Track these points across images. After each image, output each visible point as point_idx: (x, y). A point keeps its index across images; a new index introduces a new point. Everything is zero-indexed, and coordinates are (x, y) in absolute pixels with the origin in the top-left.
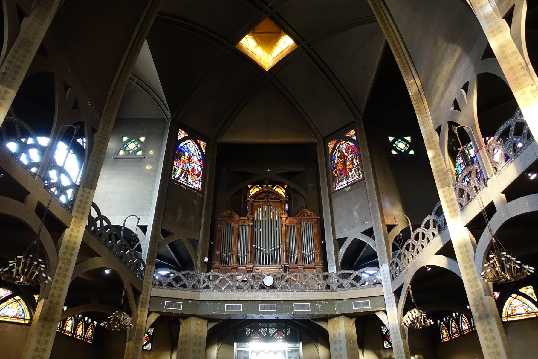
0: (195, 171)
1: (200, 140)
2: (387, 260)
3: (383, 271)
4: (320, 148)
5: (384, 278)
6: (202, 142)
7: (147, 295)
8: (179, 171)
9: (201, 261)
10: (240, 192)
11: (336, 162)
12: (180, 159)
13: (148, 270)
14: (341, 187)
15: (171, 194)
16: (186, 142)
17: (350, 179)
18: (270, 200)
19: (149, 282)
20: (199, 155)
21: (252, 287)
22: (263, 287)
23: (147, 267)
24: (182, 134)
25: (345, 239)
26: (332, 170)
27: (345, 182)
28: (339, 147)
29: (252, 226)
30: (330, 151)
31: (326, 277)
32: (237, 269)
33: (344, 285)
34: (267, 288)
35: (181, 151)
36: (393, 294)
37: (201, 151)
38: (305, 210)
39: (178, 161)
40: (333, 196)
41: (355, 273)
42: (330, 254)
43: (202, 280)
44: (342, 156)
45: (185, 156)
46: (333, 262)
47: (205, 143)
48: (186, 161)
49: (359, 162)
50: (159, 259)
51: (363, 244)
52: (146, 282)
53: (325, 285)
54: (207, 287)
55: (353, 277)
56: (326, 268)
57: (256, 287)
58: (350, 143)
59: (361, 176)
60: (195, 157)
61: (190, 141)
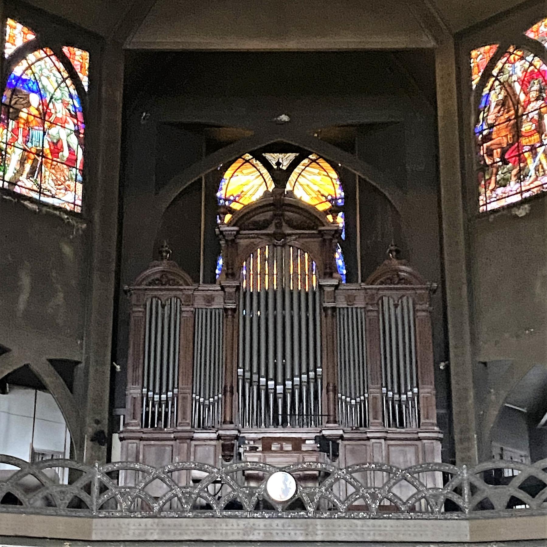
0: (61, 150)
6: (78, 52)
12: (16, 118)
14: (503, 203)
16: (31, 57)
17: (528, 180)
18: (289, 231)
20: (71, 96)
27: (513, 186)
28: (501, 71)
30: (476, 78)
38: (395, 262)
39: (12, 124)
45: (28, 105)
47: (86, 55)
53: (442, 499)
58: (538, 62)
60: (59, 105)
61: (40, 53)
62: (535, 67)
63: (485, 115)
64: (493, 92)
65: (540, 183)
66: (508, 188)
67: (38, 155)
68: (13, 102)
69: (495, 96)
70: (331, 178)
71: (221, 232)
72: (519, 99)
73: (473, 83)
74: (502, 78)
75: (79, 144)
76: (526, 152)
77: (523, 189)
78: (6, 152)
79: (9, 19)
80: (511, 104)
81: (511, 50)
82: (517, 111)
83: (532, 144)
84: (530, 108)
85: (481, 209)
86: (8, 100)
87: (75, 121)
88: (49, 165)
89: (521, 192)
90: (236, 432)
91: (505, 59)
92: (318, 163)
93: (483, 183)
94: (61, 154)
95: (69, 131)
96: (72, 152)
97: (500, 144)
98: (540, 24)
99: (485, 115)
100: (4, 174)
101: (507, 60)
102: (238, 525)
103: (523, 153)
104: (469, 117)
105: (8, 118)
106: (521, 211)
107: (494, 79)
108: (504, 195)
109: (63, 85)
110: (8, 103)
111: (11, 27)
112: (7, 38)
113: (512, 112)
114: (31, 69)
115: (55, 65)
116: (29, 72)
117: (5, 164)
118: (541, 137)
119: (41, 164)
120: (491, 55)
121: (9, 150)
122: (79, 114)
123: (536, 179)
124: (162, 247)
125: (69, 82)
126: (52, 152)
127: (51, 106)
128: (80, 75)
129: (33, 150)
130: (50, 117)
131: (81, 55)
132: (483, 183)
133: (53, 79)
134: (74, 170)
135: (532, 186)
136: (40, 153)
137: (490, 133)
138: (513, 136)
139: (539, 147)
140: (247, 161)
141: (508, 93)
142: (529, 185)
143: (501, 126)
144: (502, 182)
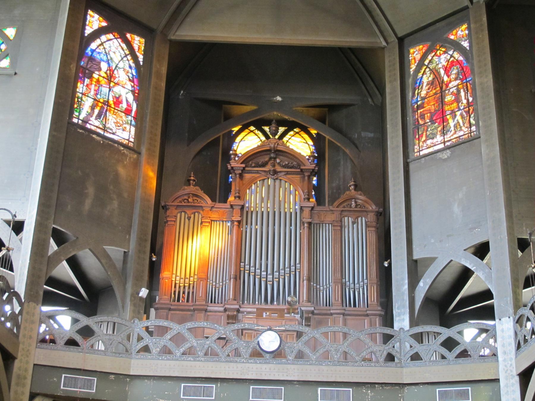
0: (121, 102)
2: (511, 310)
3: (503, 331)
7: (27, 362)
8: (88, 103)
9: (132, 295)
10: (215, 143)
11: (423, 93)
12: (91, 77)
13: (28, 313)
14: (431, 150)
16: (104, 38)
18: (278, 169)
19: (31, 337)
20: (130, 67)
21: (237, 353)
22: (258, 353)
23: (26, 305)
25: (431, 261)
26: (415, 111)
27: (439, 138)
28: (430, 61)
29: (239, 222)
30: (413, 67)
31: (387, 338)
32: (206, 311)
33: (422, 355)
34: (268, 356)
35: (91, 59)
36: (517, 379)
39: (87, 81)
40: (412, 166)
41: (446, 333)
43: (136, 336)
45: (100, 69)
46: (404, 307)
47: (143, 40)
48: (103, 81)
49: (471, 99)
50: (53, 292)
52: (24, 336)
53: (385, 353)
54: (146, 349)
56: (388, 320)
57: (245, 352)
58: (456, 55)
59: (474, 128)
60: (121, 72)
61: (110, 36)
62: (455, 58)
64: (425, 76)
65: (458, 136)
66: (435, 140)
67: (105, 104)
68: (88, 66)
70: (309, 145)
71: (232, 168)
72: (443, 80)
73: (411, 70)
74: (431, 66)
75: (134, 100)
76: (448, 115)
77: (446, 140)
78: (81, 99)
79: (89, 11)
82: (441, 88)
83: (452, 109)
84: (450, 85)
87: (133, 84)
88: (112, 112)
89: (444, 143)
90: (237, 307)
91: (434, 53)
92: (300, 135)
93: (417, 137)
94: (121, 105)
95: (128, 91)
96: (128, 105)
97: (430, 110)
98: (458, 30)
101: (435, 54)
102: (237, 368)
103: (446, 116)
104: (409, 93)
105: (84, 77)
107: (425, 67)
108: (432, 145)
109: (125, 59)
110: (85, 67)
111: (91, 16)
112: (87, 23)
113: (438, 89)
114: (103, 45)
115: (120, 45)
116: (101, 47)
117: (80, 108)
118: (458, 105)
119: (106, 111)
120: (424, 51)
121: (83, 98)
122: (135, 80)
124: (190, 177)
125: (129, 57)
126: (115, 103)
127: (115, 72)
128: (138, 54)
129: (102, 101)
130: (114, 79)
131: (139, 40)
133: (118, 54)
134: (130, 117)
135: (452, 138)
137: (423, 103)
139: (457, 111)
140: (252, 131)
141: (435, 75)
142: (450, 137)
144: (431, 136)
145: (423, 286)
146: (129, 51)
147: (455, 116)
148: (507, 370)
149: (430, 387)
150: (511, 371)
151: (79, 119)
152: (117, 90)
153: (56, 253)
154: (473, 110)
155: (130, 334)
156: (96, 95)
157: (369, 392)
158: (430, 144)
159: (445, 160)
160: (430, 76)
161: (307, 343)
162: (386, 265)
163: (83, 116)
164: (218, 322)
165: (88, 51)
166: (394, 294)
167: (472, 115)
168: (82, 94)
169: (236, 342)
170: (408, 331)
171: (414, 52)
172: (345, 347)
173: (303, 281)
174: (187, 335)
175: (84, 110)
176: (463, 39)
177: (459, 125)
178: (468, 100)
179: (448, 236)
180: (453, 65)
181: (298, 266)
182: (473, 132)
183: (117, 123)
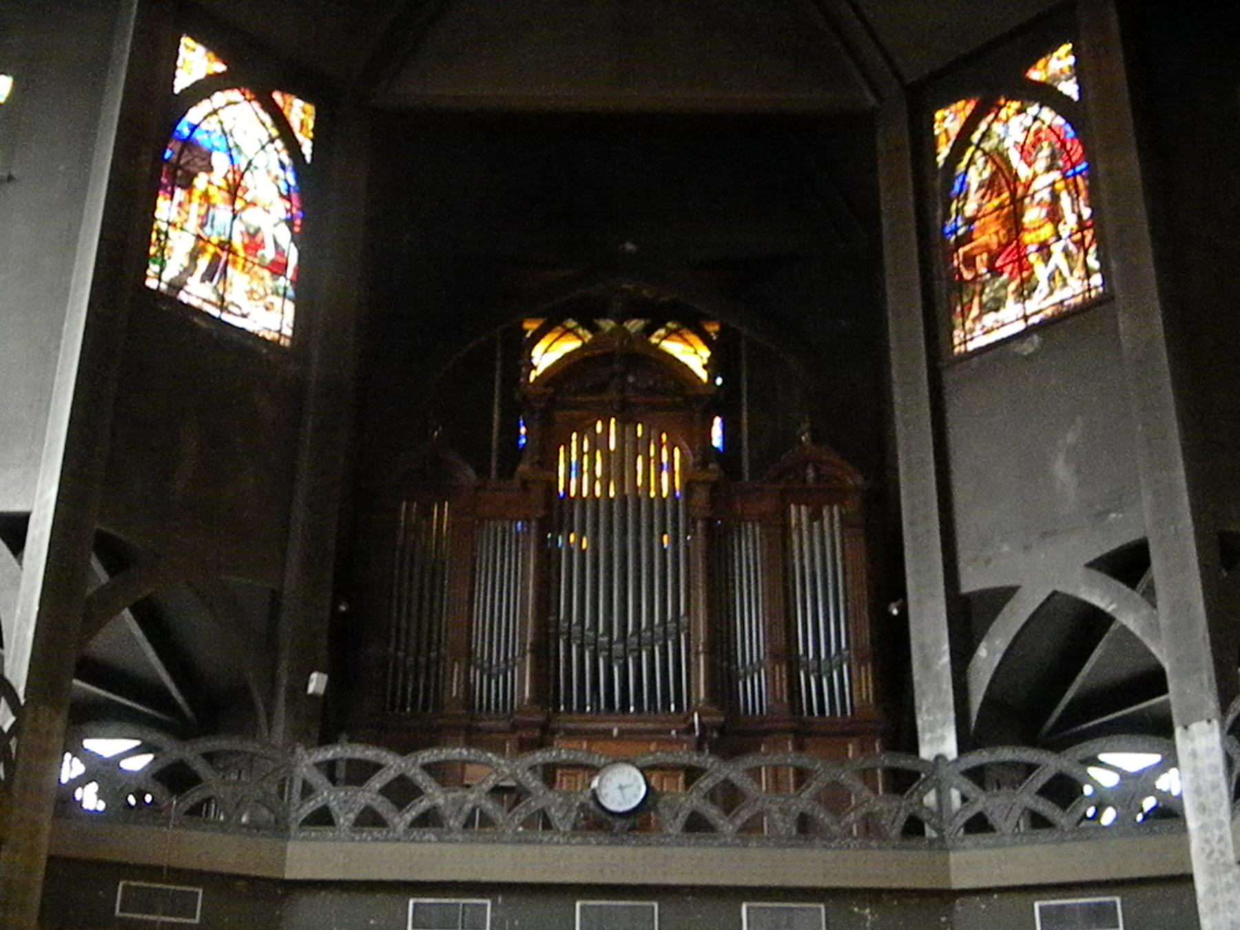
0: (261, 245)
1: (285, 90)
2: (1212, 705)
3: (1194, 754)
4: (891, 138)
5: (1198, 791)
6: (298, 104)
11: (970, 209)
12: (188, 186)
15: (144, 354)
16: (219, 98)
17: (1037, 296)
20: (283, 166)
24: (194, 62)
28: (985, 135)
30: (944, 151)
33: (995, 818)
35: (189, 143)
37: (293, 146)
39: (180, 194)
40: (949, 378)
41: (1051, 764)
42: (927, 666)
43: (298, 785)
44: (1002, 177)
45: (209, 169)
46: (942, 706)
48: (219, 197)
51: (1093, 623)
53: (903, 817)
54: (323, 818)
55: (1040, 779)
56: (904, 737)
58: (1047, 115)
59: (1096, 280)
61: (235, 95)
62: (1043, 122)
63: (961, 204)
64: (972, 169)
67: (223, 249)
68: (182, 162)
69: (977, 174)
74: (986, 146)
75: (293, 240)
80: (1003, 182)
81: (1002, 102)
83: (1042, 238)
84: (1035, 186)
85: (957, 350)
86: (175, 157)
87: (288, 205)
89: (1026, 318)
91: (991, 116)
93: (959, 309)
94: (260, 252)
99: (961, 204)
100: (162, 270)
104: (935, 211)
106: (1025, 345)
108: (995, 325)
109: (270, 147)
111: (187, 47)
113: (1006, 195)
116: (214, 119)
117: (163, 255)
118: (1056, 227)
119: (226, 263)
122: (294, 196)
123: (1051, 292)
125: (279, 144)
126: (246, 247)
127: (247, 175)
132: (959, 309)
136: (226, 246)
138: (1009, 231)
143: (988, 218)
145: (988, 656)
146: (278, 129)
147: (1049, 255)
148: (1212, 852)
149: (1017, 899)
150: (1222, 853)
151: (160, 279)
152: (252, 217)
153: (101, 590)
154: (1094, 236)
155: (284, 780)
156: (202, 226)
157: (868, 911)
158: (987, 326)
159: (1029, 358)
160: (984, 168)
161: (711, 796)
162: (895, 612)
163: (170, 273)
164: (499, 749)
165: (183, 128)
166: (916, 678)
167: (1092, 250)
168: (169, 223)
169: (541, 797)
170: (956, 761)
171: (944, 119)
172: (804, 802)
173: (697, 654)
174: (421, 779)
175: (174, 263)
176: (1063, 77)
177: (1060, 273)
178: (1080, 216)
179: (1044, 535)
180: (1039, 140)
181: (684, 620)
182: (1096, 287)
183: (252, 292)
